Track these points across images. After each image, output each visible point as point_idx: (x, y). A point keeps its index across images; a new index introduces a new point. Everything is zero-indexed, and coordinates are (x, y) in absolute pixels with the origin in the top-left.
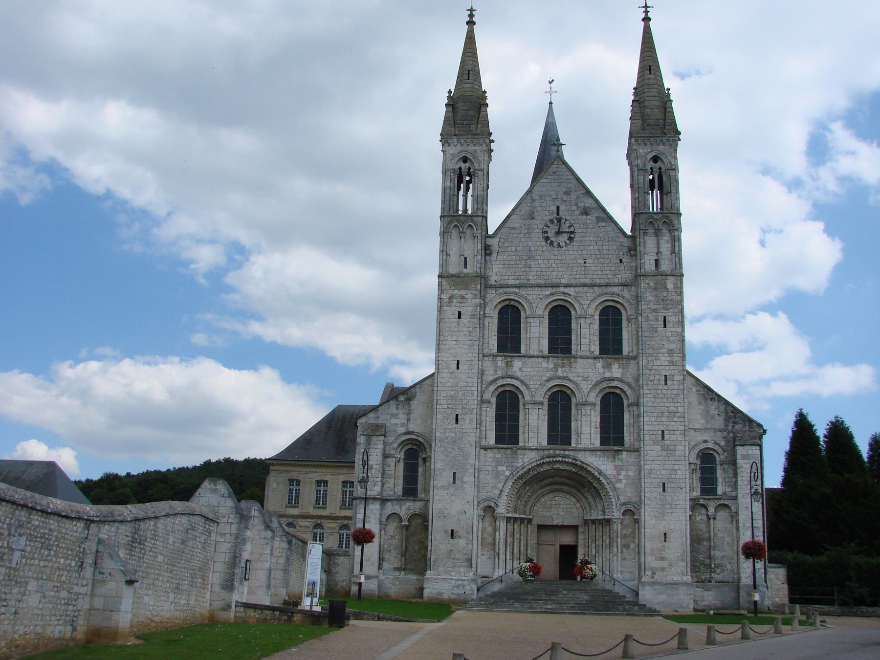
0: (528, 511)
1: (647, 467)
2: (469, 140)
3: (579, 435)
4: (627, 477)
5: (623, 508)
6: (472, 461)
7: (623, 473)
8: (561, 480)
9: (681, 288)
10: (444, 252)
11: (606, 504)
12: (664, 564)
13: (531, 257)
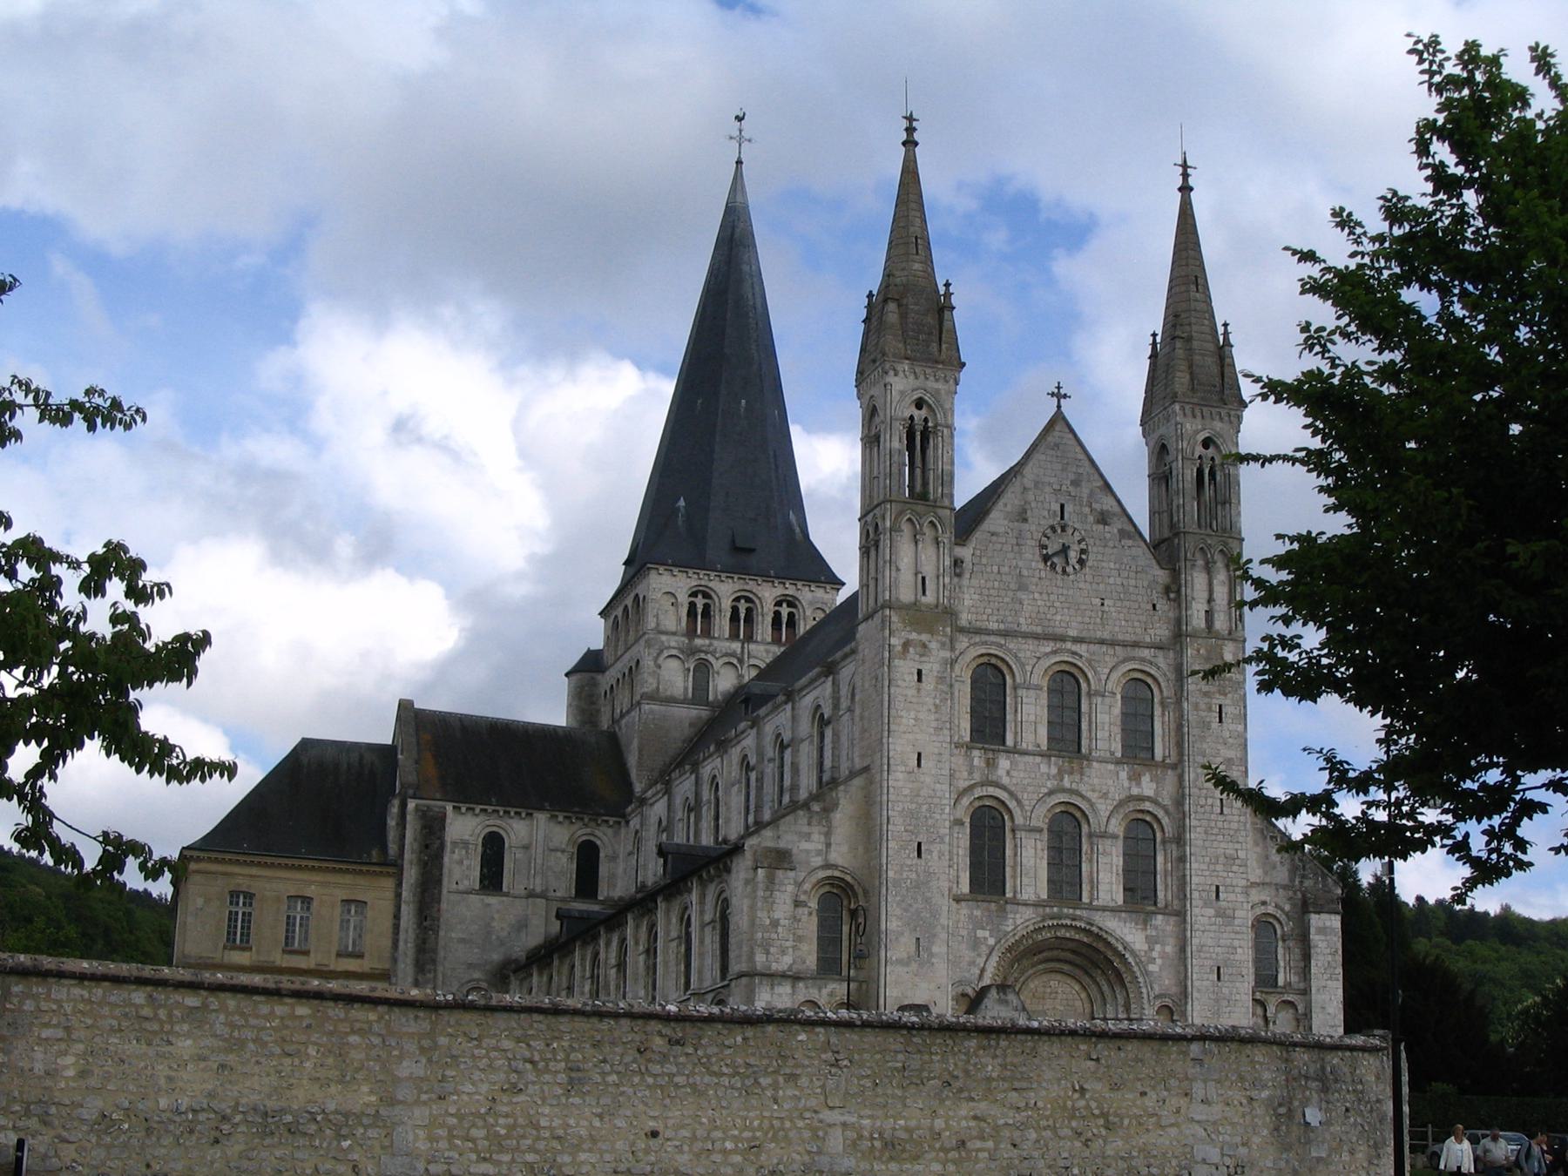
2: (928, 371)
3: (1094, 885)
4: (1163, 955)
5: (1158, 1003)
7: (1158, 947)
13: (1022, 587)
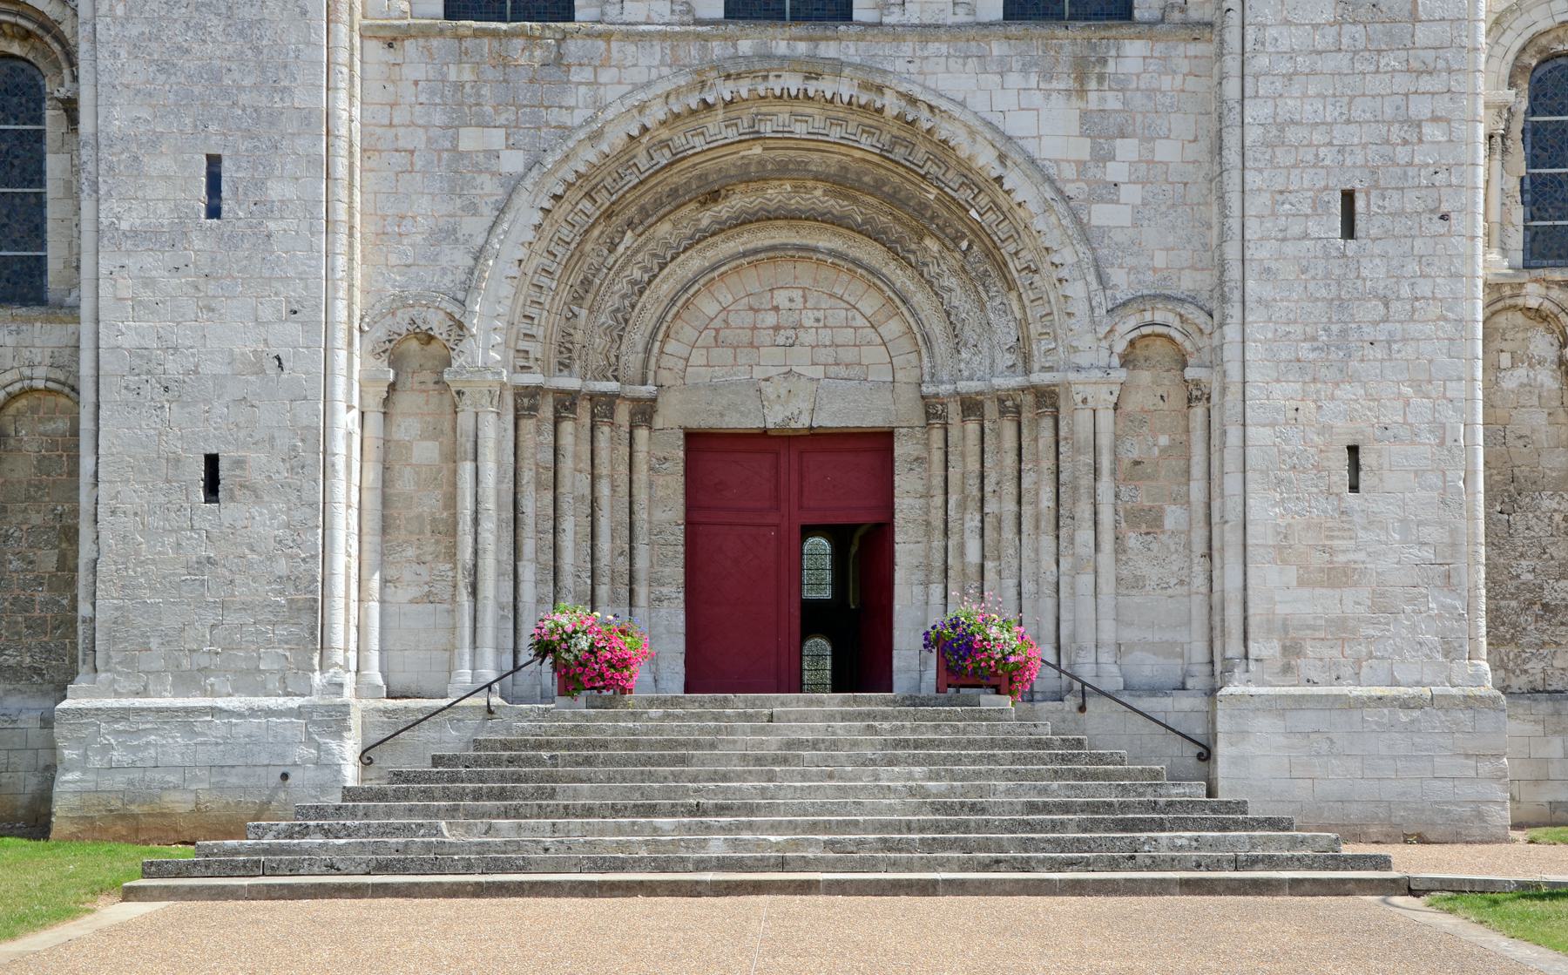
0: (632, 361)
1: (1256, 111)
5: (1127, 326)
7: (1127, 149)
11: (1034, 312)
12: (1352, 602)
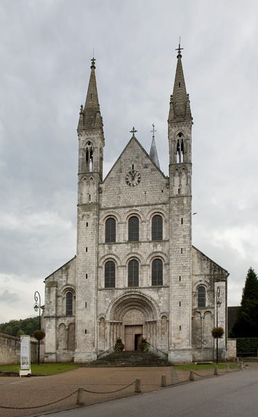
4: (164, 300)
5: (162, 315)
6: (94, 296)
7: (162, 298)
8: (134, 304)
9: (190, 203)
10: (80, 193)
12: (180, 341)
13: (120, 193)
